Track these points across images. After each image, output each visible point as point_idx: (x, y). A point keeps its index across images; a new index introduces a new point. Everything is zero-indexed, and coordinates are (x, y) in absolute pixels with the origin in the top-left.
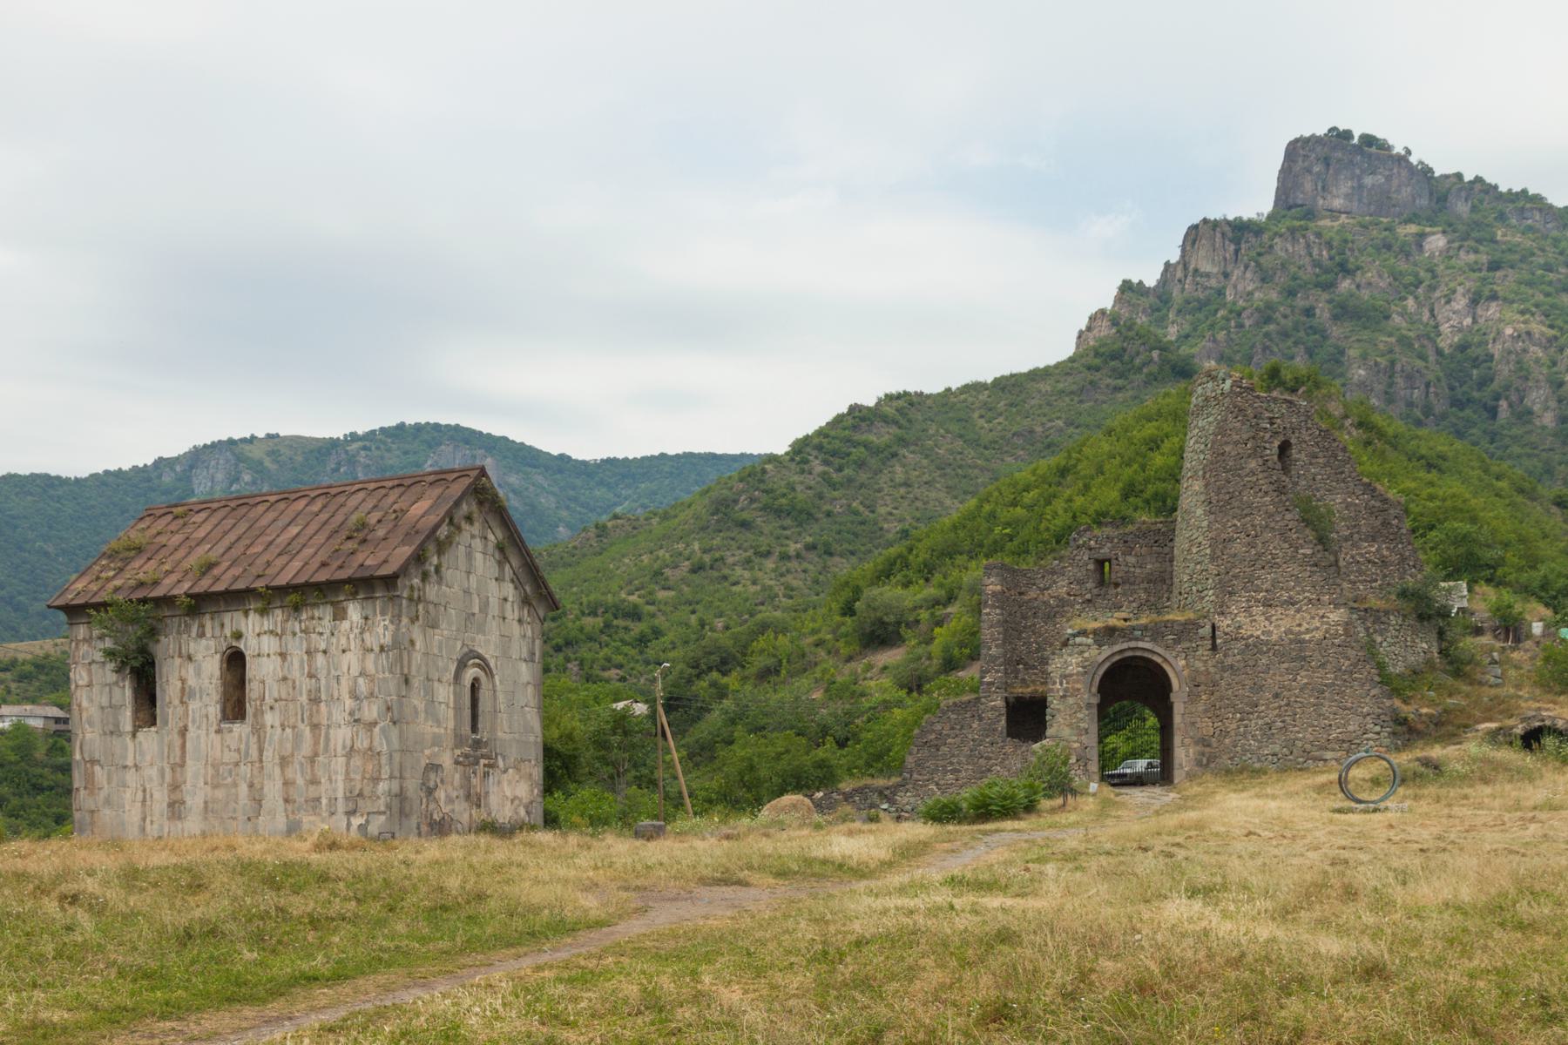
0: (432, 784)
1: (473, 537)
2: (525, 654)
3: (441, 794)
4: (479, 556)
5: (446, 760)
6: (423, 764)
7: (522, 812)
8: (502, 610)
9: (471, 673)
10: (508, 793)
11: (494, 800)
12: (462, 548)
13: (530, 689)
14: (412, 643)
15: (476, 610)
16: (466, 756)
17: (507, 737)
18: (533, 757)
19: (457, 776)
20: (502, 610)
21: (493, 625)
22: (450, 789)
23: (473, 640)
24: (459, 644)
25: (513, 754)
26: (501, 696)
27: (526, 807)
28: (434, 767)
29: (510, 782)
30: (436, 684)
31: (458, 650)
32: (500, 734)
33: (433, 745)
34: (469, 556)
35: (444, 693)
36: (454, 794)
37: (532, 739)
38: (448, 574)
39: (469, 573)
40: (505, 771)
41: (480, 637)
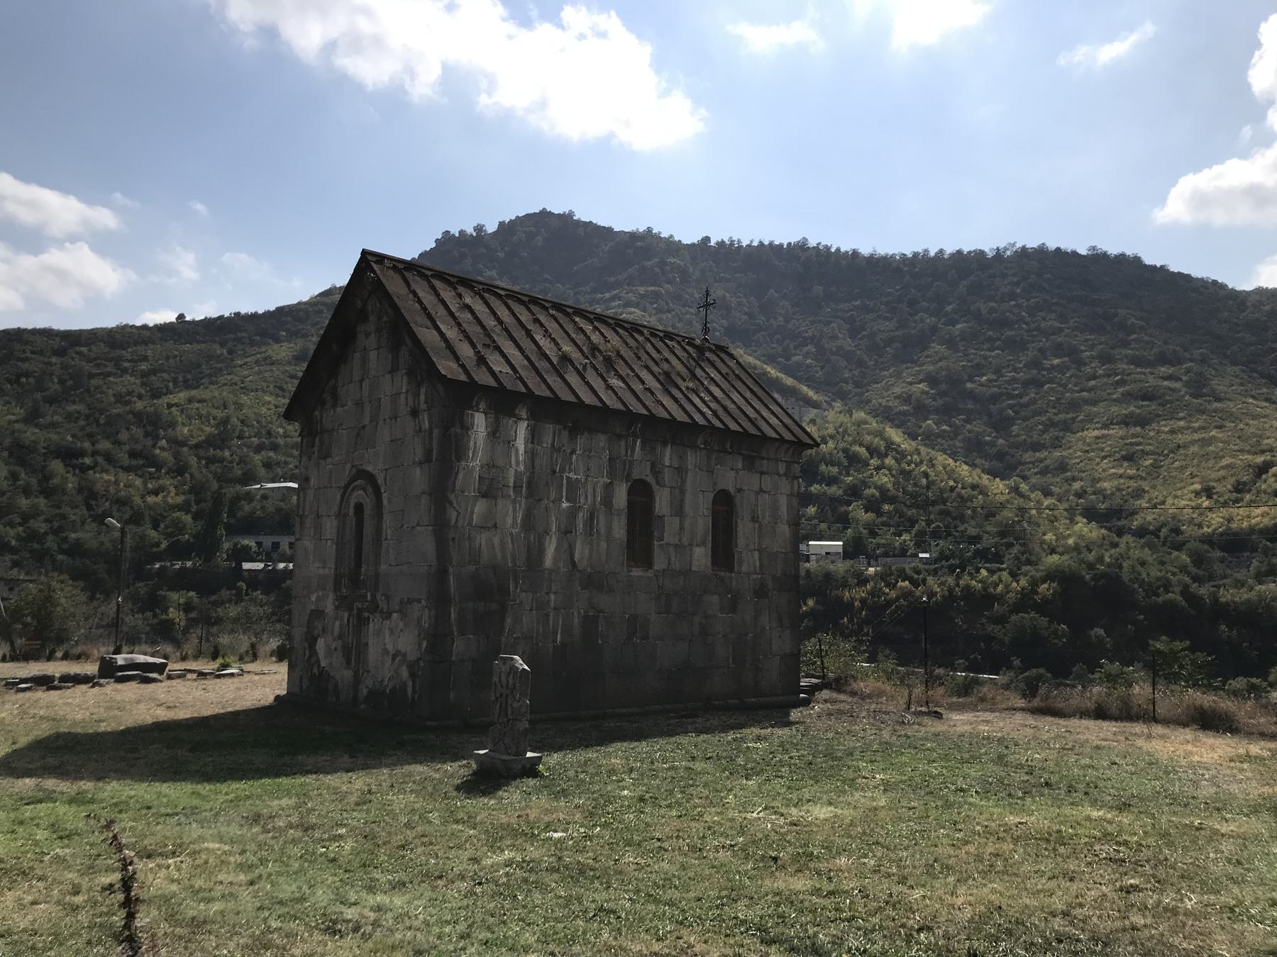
1: (367, 335)
2: (419, 454)
3: (321, 645)
4: (373, 355)
5: (329, 606)
7: (405, 673)
9: (358, 496)
10: (390, 647)
11: (373, 654)
12: (357, 355)
13: (425, 500)
15: (366, 421)
19: (337, 624)
24: (348, 466)
26: (387, 519)
27: (411, 666)
28: (318, 614)
29: (392, 632)
34: (365, 360)
39: (361, 381)
40: (388, 616)
41: (371, 451)
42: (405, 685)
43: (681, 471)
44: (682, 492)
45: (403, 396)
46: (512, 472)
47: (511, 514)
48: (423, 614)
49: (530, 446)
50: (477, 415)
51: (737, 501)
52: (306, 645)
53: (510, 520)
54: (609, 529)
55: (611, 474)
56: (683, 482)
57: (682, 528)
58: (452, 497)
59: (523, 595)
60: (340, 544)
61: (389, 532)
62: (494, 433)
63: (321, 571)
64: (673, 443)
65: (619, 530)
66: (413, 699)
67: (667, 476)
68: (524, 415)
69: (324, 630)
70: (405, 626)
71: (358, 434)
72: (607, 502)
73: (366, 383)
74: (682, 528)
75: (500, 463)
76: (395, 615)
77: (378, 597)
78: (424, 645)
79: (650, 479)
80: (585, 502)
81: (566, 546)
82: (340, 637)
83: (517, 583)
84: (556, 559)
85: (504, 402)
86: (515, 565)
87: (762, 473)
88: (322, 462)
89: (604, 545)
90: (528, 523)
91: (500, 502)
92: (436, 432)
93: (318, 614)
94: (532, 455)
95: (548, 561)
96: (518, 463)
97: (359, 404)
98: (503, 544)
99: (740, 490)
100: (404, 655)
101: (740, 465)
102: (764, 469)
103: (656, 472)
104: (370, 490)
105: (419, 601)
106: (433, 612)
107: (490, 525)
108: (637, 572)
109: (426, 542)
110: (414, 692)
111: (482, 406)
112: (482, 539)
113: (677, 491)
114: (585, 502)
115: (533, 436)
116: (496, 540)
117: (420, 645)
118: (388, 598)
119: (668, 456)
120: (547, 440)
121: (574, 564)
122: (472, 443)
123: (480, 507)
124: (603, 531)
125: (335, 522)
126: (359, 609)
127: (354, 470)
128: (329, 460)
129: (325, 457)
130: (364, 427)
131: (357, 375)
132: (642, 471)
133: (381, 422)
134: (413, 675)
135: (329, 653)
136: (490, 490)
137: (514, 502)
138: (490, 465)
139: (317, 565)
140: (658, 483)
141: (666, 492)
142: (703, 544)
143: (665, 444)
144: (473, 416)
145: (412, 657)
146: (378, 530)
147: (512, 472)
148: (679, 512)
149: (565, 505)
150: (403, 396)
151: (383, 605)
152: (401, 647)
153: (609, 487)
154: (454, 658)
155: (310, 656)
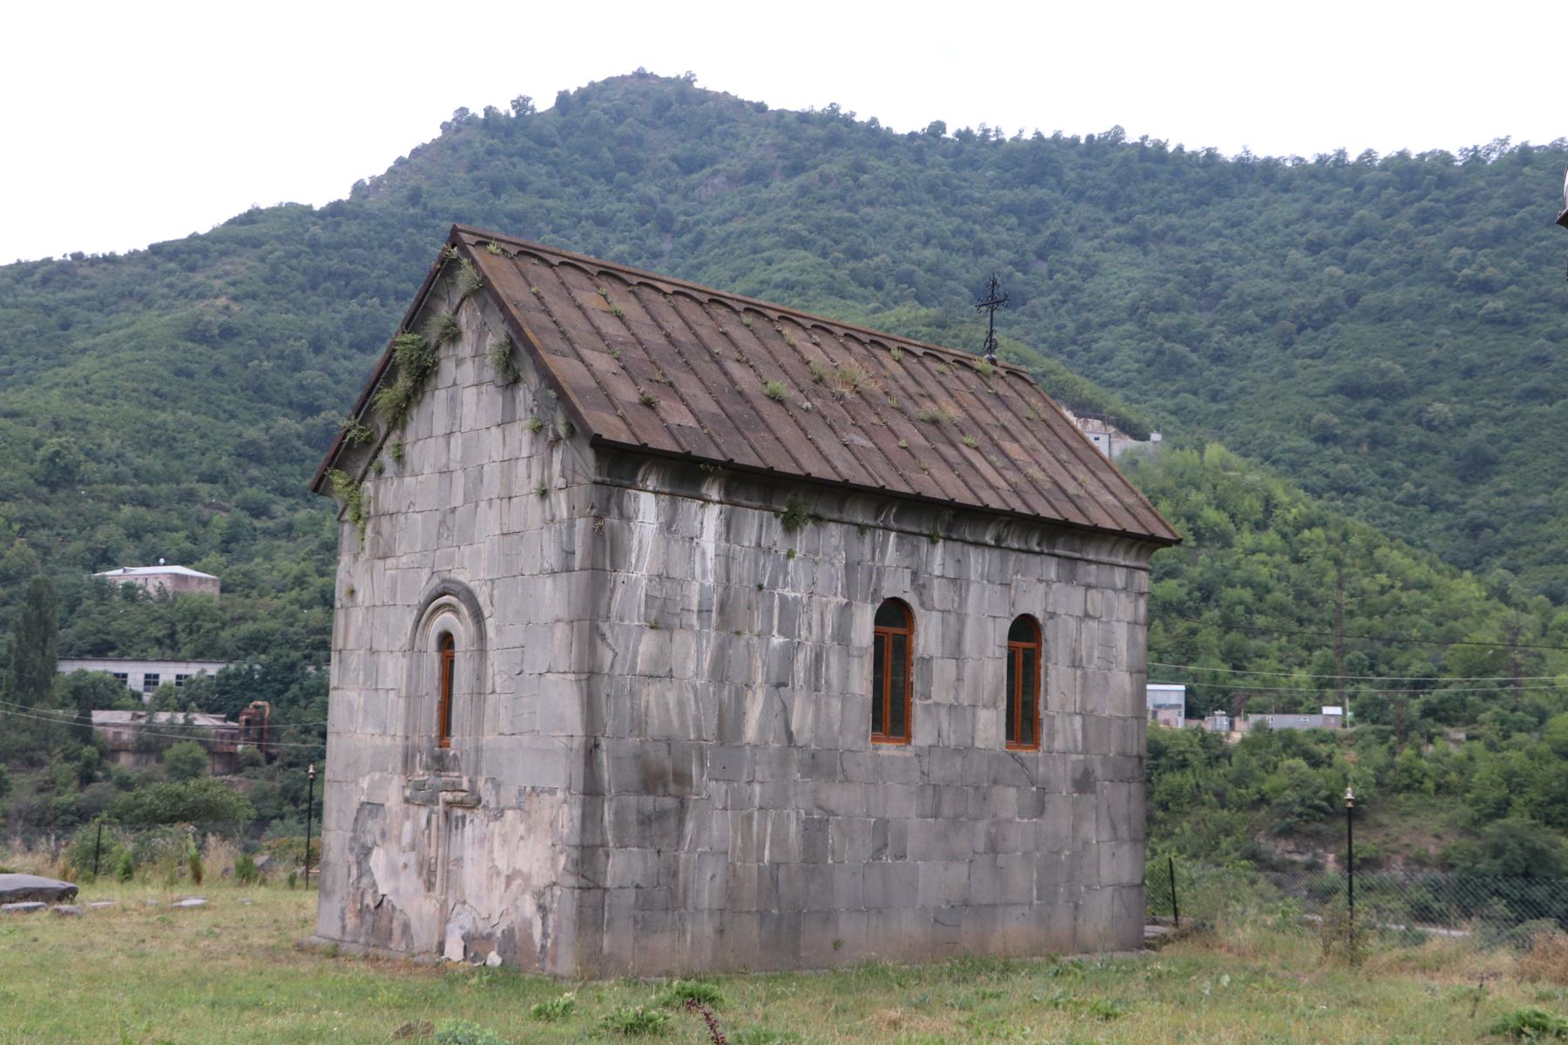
0: (369, 840)
1: (459, 363)
3: (378, 860)
4: (469, 395)
5: (393, 796)
6: (356, 806)
7: (528, 907)
8: (507, 481)
10: (502, 864)
11: (472, 875)
12: (441, 395)
13: (561, 631)
14: (352, 592)
15: (458, 500)
16: (419, 787)
17: (506, 742)
18: (560, 784)
19: (408, 826)
20: (507, 481)
21: (489, 522)
22: (393, 848)
23: (451, 560)
25: (520, 774)
26: (495, 660)
27: (540, 894)
28: (372, 808)
29: (505, 840)
30: (383, 657)
31: (424, 584)
32: (488, 738)
33: (373, 769)
34: (453, 401)
35: (394, 669)
36: (401, 861)
37: (560, 743)
38: (413, 453)
40: (499, 814)
41: (466, 550)
42: (528, 924)
43: (958, 583)
44: (961, 619)
45: (521, 466)
46: (696, 587)
47: (693, 654)
48: (565, 815)
49: (723, 544)
50: (643, 495)
51: (1048, 632)
52: (352, 858)
53: (692, 666)
54: (846, 676)
55: (849, 591)
56: (963, 602)
57: (959, 679)
58: (605, 627)
59: (712, 784)
60: (412, 698)
61: (498, 680)
62: (668, 526)
63: (378, 741)
64: (947, 539)
65: (861, 682)
66: (543, 947)
67: (938, 592)
68: (715, 494)
69: (383, 835)
70: (529, 830)
71: (442, 523)
72: (842, 636)
73: (456, 441)
74: (959, 679)
75: (677, 573)
76: (509, 814)
77: (481, 783)
78: (562, 860)
79: (911, 598)
80: (808, 638)
81: (777, 706)
82: (413, 847)
83: (702, 766)
84: (762, 729)
85: (685, 473)
86: (700, 738)
87: (1088, 587)
88: (380, 564)
89: (836, 705)
90: (720, 672)
91: (678, 636)
92: (581, 524)
93: (372, 808)
94: (727, 560)
95: (751, 732)
96: (704, 575)
97: (446, 472)
98: (681, 704)
99: (1052, 615)
100: (527, 879)
101: (1053, 575)
102: (1092, 580)
103: (920, 587)
104: (464, 609)
105: (552, 791)
106: (577, 812)
107: (662, 673)
108: (888, 749)
109: (564, 699)
110: (545, 935)
111: (651, 483)
112: (650, 694)
113: (952, 618)
114: (808, 638)
115: (729, 528)
116: (671, 697)
117: (554, 860)
118: (497, 786)
119: (938, 558)
120: (750, 536)
121: (790, 735)
122: (635, 542)
123: (648, 643)
124: (835, 682)
125: (404, 662)
126: (449, 804)
127: (436, 581)
128: (390, 562)
129: (385, 557)
130: (453, 510)
131: (440, 427)
132: (897, 585)
133: (483, 504)
134: (542, 909)
135: (393, 872)
136: (661, 621)
137: (699, 635)
138: (662, 578)
139: (370, 730)
140: (922, 604)
141: (936, 616)
142: (995, 705)
143: (933, 540)
144: (636, 497)
145: (539, 881)
146: (480, 677)
147: (696, 587)
148: (956, 652)
149: (777, 640)
150: (522, 464)
151: (488, 795)
152: (522, 864)
153: (845, 610)
154: (608, 884)
155: (360, 877)
